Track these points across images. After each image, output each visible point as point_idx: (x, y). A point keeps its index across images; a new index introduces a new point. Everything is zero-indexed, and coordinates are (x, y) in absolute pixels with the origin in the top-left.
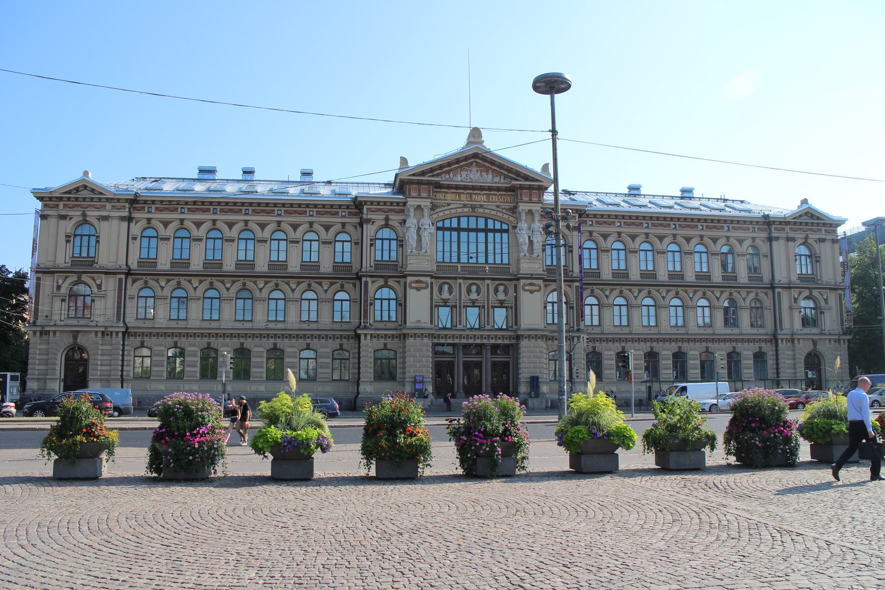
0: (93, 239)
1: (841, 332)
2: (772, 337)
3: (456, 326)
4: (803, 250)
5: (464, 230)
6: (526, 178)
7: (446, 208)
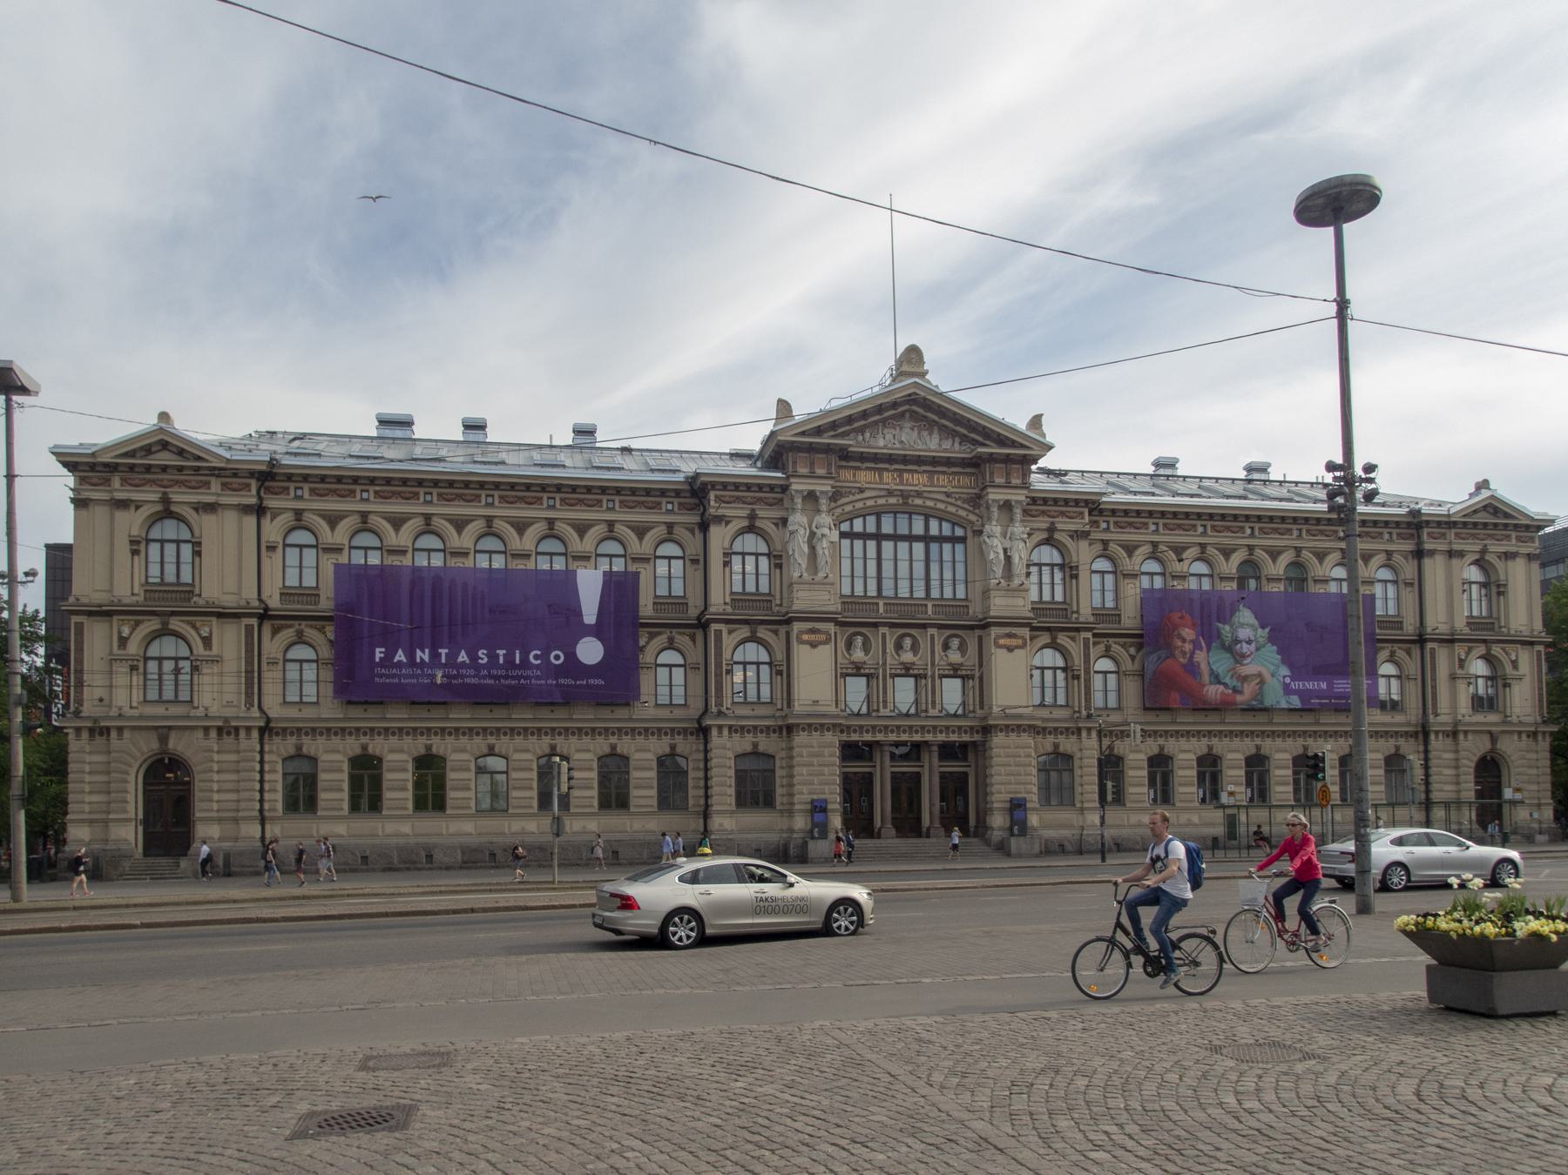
0: (186, 550)
1: (1539, 719)
2: (1419, 729)
3: (878, 711)
4: (1474, 574)
5: (888, 537)
6: (1002, 441)
7: (858, 497)
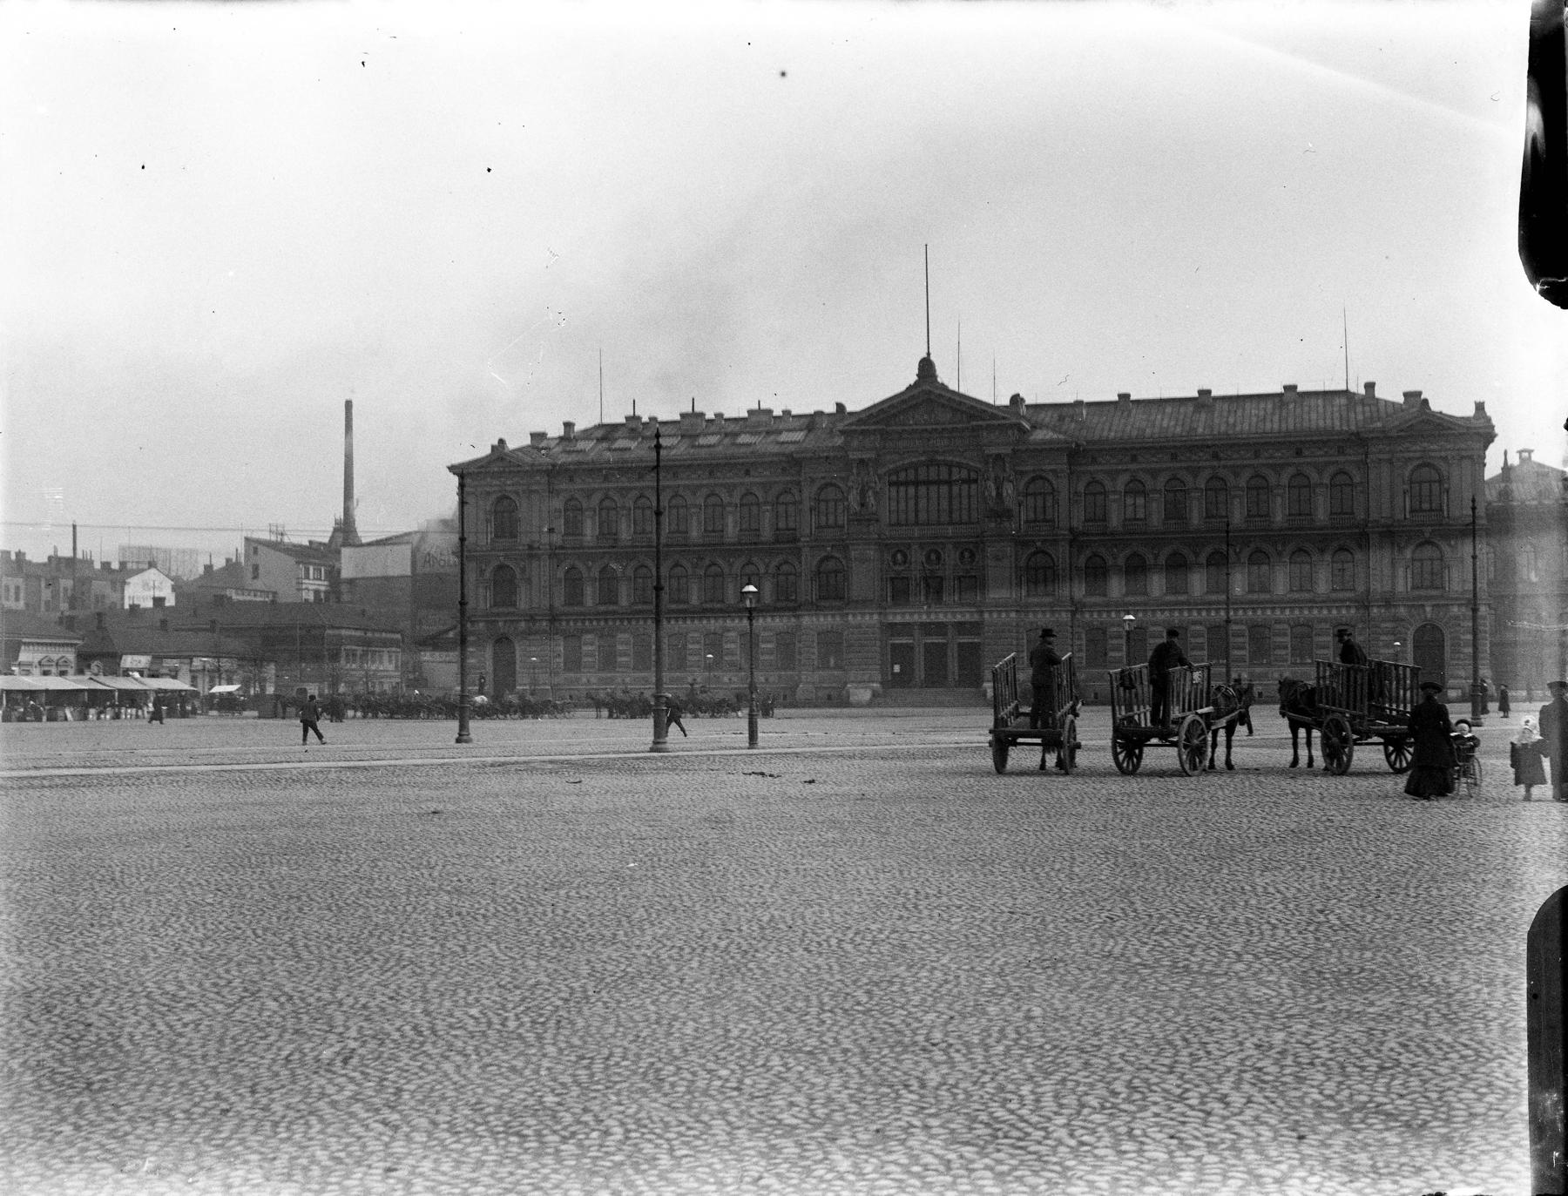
6: (994, 416)
